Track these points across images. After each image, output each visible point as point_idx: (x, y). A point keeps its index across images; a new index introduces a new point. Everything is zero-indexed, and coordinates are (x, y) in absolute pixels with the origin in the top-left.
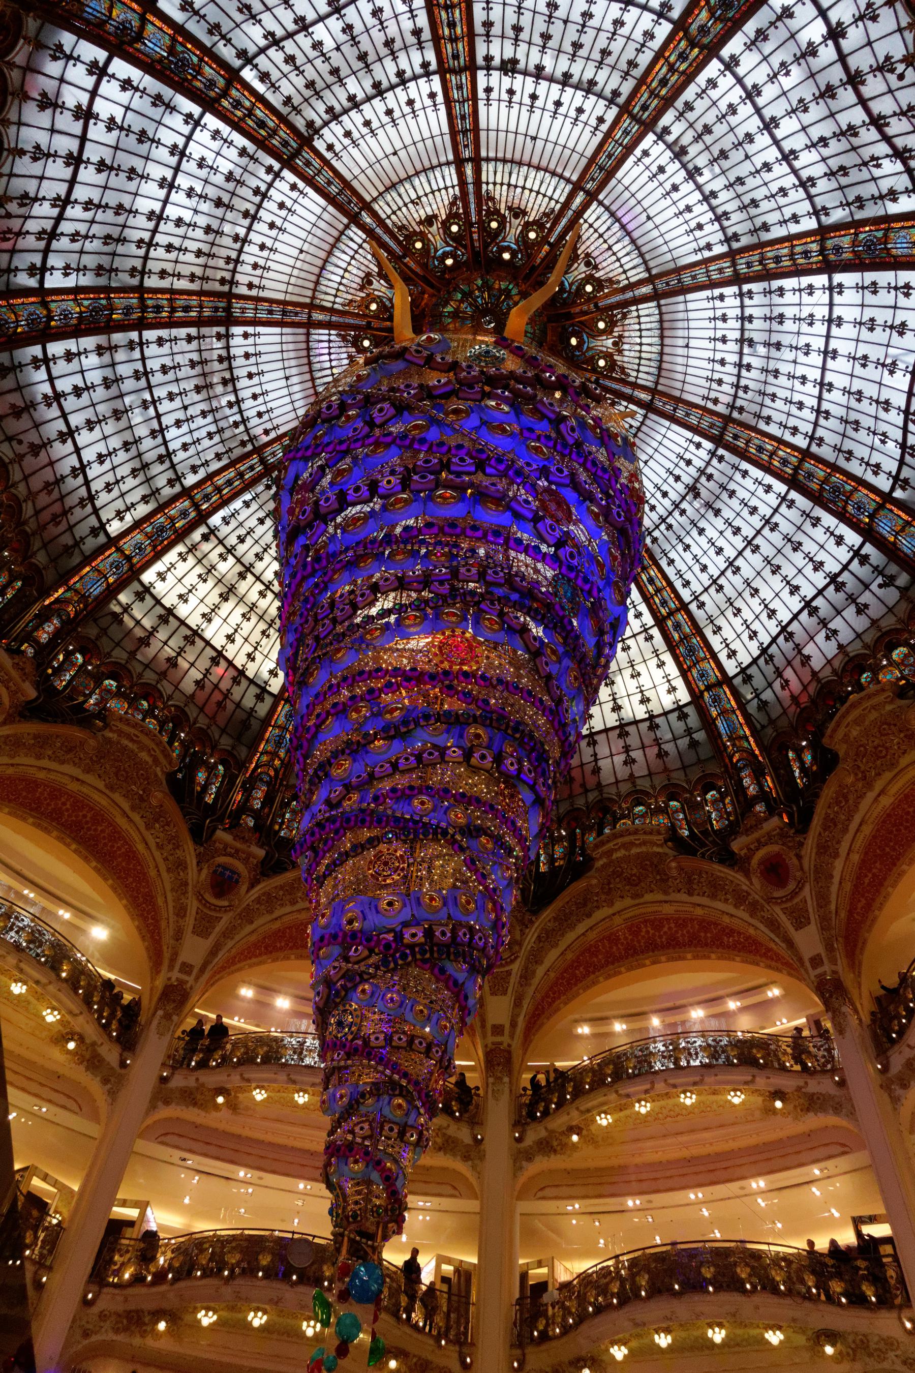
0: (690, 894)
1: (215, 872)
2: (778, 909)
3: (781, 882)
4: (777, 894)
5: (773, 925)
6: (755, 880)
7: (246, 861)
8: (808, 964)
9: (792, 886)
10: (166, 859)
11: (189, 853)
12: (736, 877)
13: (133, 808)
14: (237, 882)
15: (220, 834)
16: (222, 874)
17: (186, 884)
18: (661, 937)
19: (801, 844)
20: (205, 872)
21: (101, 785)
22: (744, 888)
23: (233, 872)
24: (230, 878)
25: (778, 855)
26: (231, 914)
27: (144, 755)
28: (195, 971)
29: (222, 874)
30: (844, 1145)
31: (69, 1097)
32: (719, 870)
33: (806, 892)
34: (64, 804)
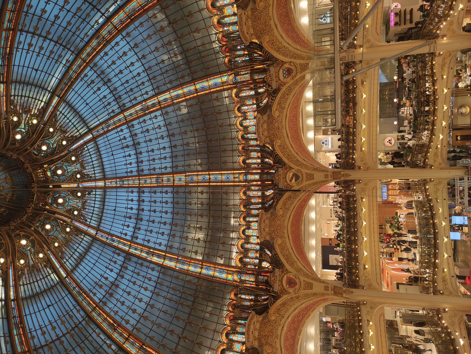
0: (283, 317)
2: (302, 291)
3: (295, 284)
4: (297, 287)
5: (307, 296)
6: (291, 290)
8: (326, 292)
9: (297, 281)
12: (284, 298)
18: (291, 341)
19: (287, 270)
22: (289, 297)
25: (287, 278)
30: (381, 315)
32: (279, 302)
33: (302, 278)
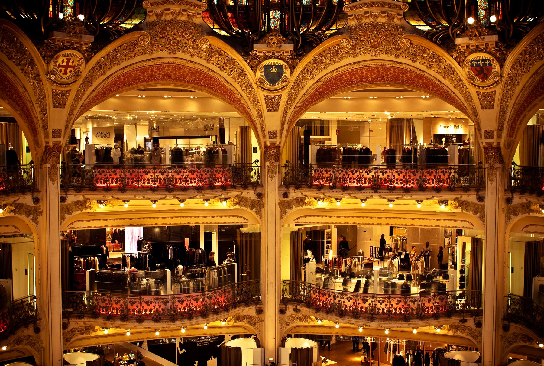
1: (472, 65)
7: (485, 50)
10: (438, 73)
11: (449, 60)
13: (397, 56)
14: (490, 65)
15: (459, 41)
16: (478, 65)
17: (461, 80)
20: (466, 69)
21: (368, 57)
23: (484, 60)
24: (485, 65)
26: (501, 86)
27: (381, 20)
28: (495, 135)
29: (478, 65)
31: (464, 221)
34: (362, 73)
